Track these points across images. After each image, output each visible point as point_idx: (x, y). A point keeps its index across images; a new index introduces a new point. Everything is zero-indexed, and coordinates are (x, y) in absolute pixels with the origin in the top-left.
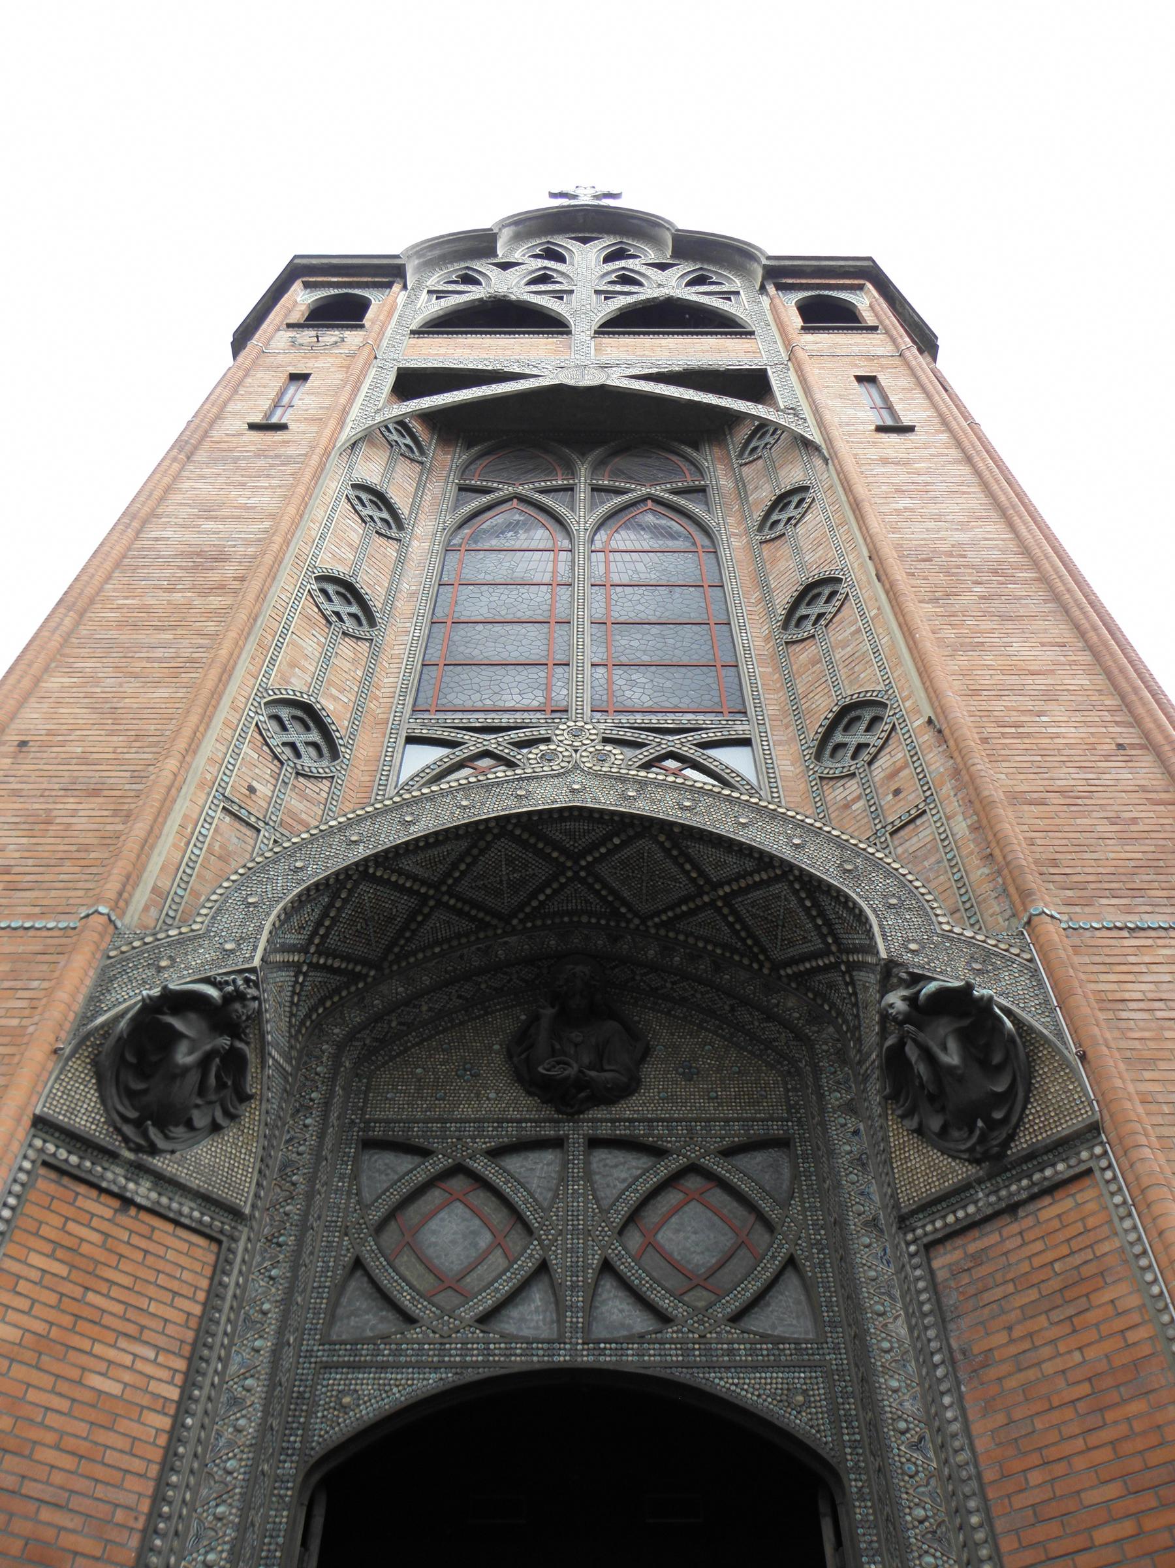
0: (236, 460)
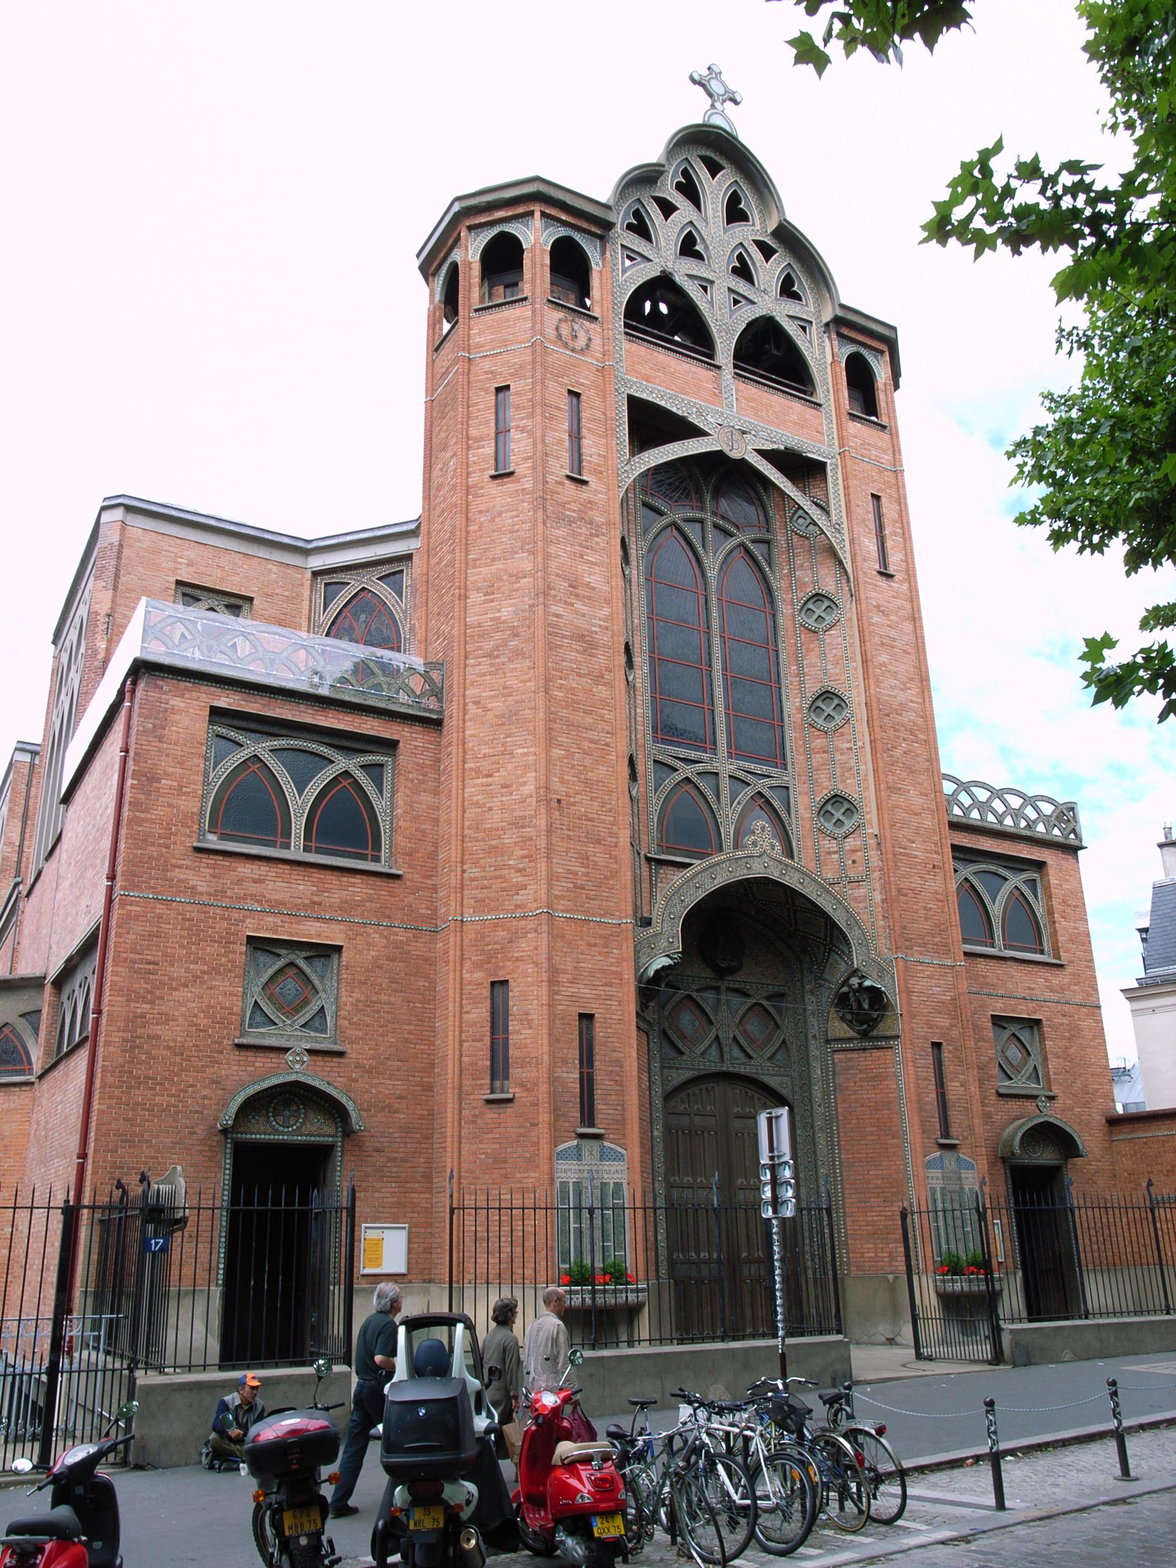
0: (572, 521)
